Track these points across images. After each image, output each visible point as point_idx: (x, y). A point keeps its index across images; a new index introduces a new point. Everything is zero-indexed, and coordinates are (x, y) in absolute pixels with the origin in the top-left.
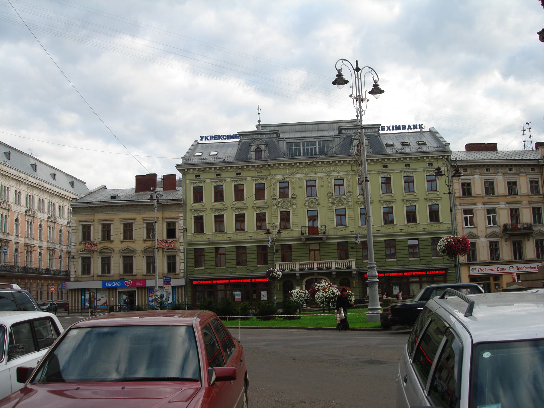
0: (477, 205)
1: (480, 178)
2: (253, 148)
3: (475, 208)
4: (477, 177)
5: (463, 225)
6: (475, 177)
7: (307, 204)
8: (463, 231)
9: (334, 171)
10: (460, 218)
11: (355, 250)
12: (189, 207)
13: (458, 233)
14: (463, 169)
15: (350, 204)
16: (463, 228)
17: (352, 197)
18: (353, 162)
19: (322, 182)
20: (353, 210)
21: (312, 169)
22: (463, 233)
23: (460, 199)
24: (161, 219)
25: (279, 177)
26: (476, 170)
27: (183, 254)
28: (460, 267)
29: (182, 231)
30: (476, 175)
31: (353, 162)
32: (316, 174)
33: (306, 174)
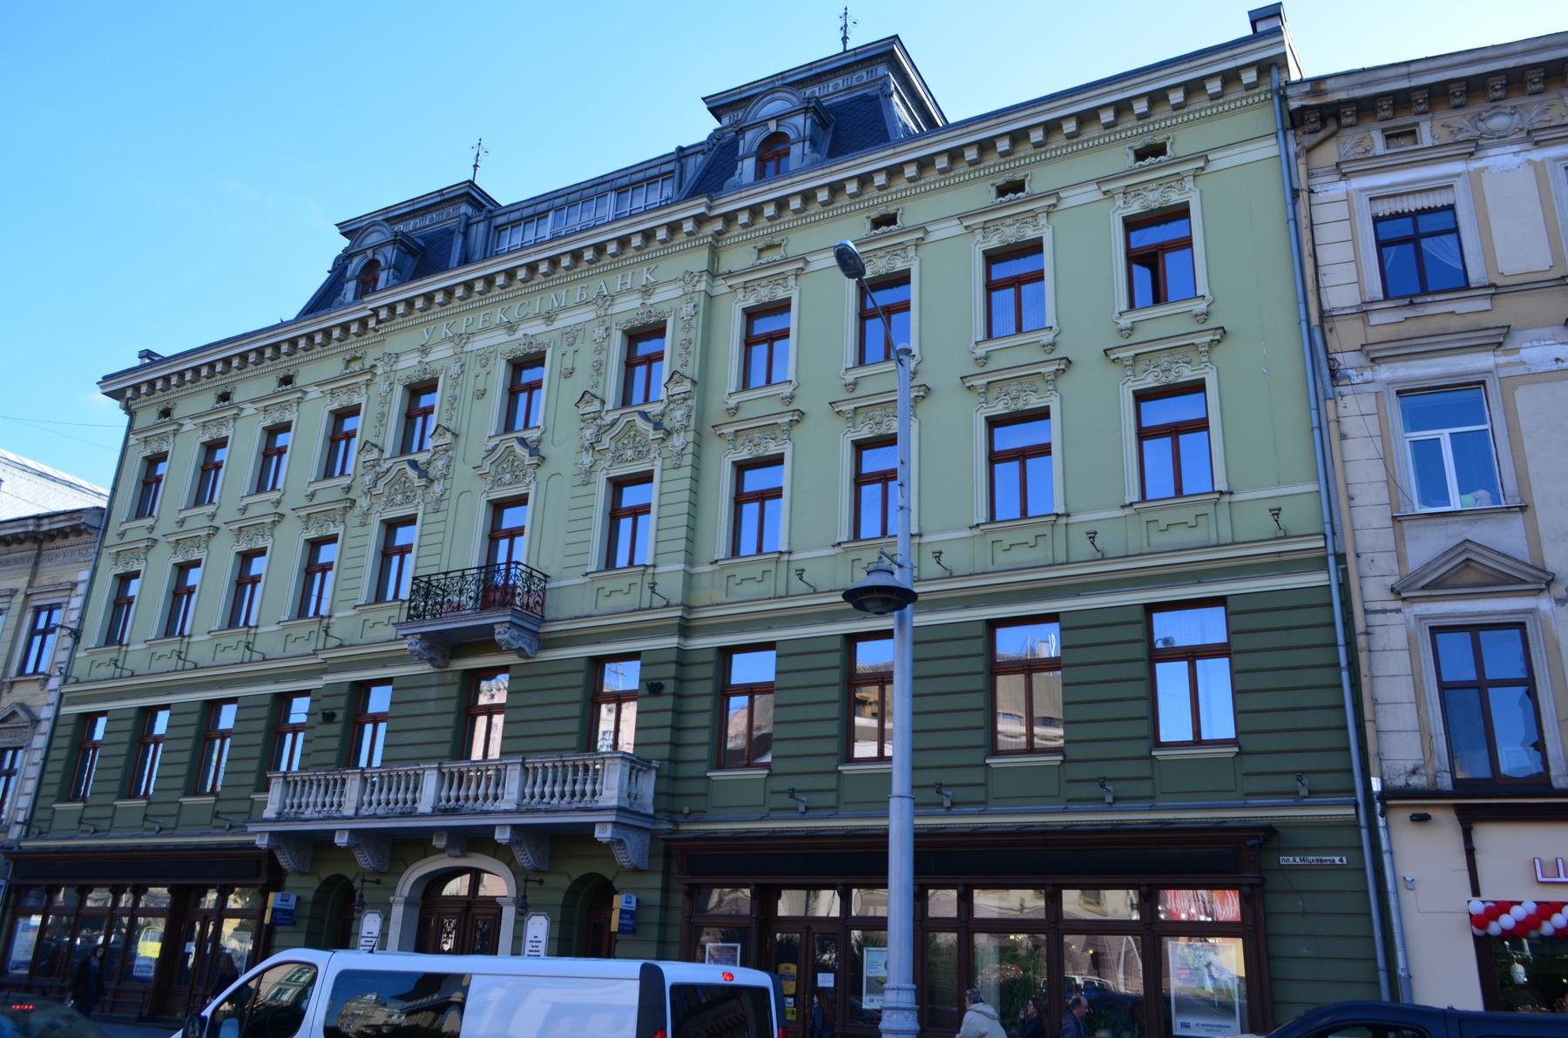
0: (1517, 350)
1: (1529, 162)
2: (356, 264)
3: (1503, 373)
4: (1503, 162)
5: (1393, 503)
6: (1474, 165)
7: (487, 467)
8: (1400, 540)
9: (630, 291)
10: (1374, 448)
11: (667, 702)
12: (111, 538)
13: (1351, 559)
14: (1390, 137)
15: (677, 441)
16: (1394, 518)
17: (690, 402)
18: (718, 225)
19: (570, 355)
20: (687, 471)
21: (537, 304)
22: (1401, 559)
23: (1366, 323)
24: (19, 598)
25: (409, 366)
26: (1490, 117)
27: (40, 741)
28: (1381, 822)
29: (68, 642)
30: (1491, 152)
31: (718, 225)
32: (549, 318)
33: (511, 328)
